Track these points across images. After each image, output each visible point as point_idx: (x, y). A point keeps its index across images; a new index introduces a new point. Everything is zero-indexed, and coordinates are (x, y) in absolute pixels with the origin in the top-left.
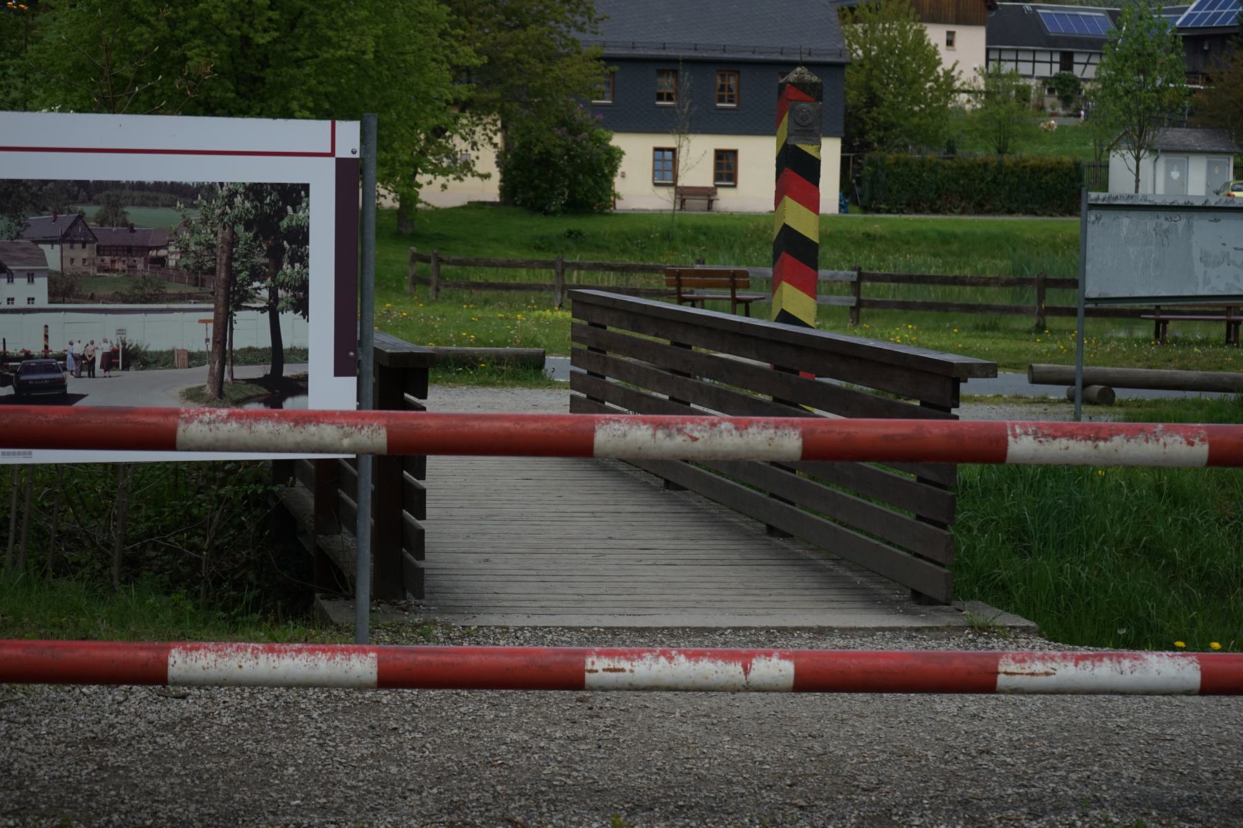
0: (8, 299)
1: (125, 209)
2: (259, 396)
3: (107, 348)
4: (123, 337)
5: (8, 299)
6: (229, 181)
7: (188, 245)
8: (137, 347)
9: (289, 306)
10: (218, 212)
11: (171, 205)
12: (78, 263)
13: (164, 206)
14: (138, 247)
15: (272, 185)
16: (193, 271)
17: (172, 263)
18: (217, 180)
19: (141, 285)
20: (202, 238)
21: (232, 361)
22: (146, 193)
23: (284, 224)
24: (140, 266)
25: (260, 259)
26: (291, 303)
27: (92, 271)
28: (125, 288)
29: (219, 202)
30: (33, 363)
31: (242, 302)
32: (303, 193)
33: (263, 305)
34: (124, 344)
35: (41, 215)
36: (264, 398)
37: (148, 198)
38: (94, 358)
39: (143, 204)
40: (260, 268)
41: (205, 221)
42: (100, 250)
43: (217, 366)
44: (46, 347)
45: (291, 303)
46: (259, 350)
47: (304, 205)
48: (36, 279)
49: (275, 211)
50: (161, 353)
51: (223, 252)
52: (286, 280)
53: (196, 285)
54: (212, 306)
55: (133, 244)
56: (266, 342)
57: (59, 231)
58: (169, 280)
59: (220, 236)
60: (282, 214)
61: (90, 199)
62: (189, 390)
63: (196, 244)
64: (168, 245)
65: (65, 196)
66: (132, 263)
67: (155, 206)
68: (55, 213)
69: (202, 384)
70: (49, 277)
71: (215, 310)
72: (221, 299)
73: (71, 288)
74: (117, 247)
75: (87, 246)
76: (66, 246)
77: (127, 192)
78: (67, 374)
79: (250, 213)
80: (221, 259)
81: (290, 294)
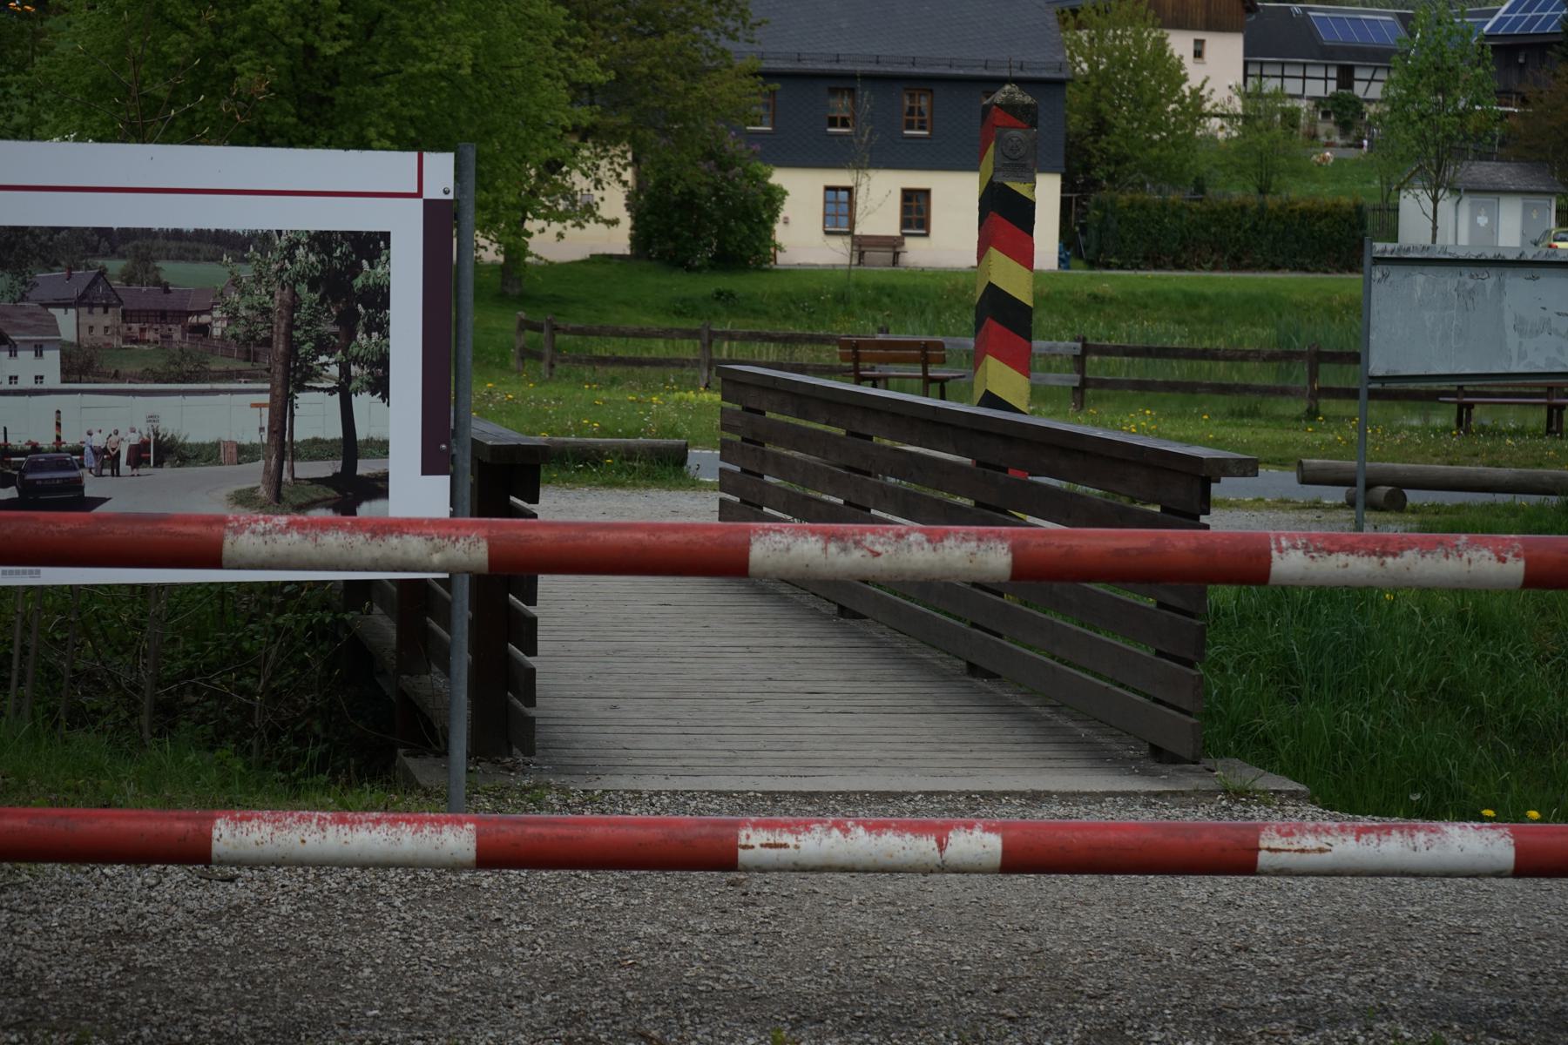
0: (11, 378)
1: (158, 264)
2: (326, 499)
3: (135, 439)
4: (155, 425)
5: (11, 378)
6: (289, 228)
7: (237, 309)
8: (173, 438)
9: (364, 386)
10: (275, 267)
11: (216, 258)
12: (98, 332)
13: (207, 260)
14: (174, 311)
15: (343, 233)
16: (244, 342)
17: (217, 332)
18: (274, 228)
19: (178, 360)
20: (255, 301)
21: (293, 456)
22: (185, 244)
23: (359, 282)
24: (177, 336)
25: (328, 327)
26: (368, 383)
27: (117, 342)
28: (158, 364)
29: (276, 255)
30: (41, 458)
31: (305, 381)
32: (382, 243)
33: (332, 384)
34: (157, 434)
35: (52, 271)
36: (333, 502)
37: (186, 250)
38: (119, 452)
39: (180, 258)
40: (328, 338)
41: (258, 280)
42: (127, 316)
43: (273, 462)
44: (58, 438)
45: (368, 383)
46: (327, 442)
47: (383, 258)
48: (45, 353)
49: (346, 266)
50: (203, 446)
51: (282, 318)
52: (361, 354)
53: (247, 360)
54: (268, 386)
55: (168, 308)
56: (336, 432)
57: (75, 291)
58: (213, 353)
59: (277, 297)
60: (355, 270)
61: (113, 252)
62: (239, 492)
63: (247, 307)
64: (212, 309)
65: (82, 247)
66: (167, 332)
67: (196, 260)
68: (70, 269)
69: (255, 485)
70: (61, 350)
71: (271, 391)
72: (279, 378)
73: (90, 363)
74: (147, 311)
75: (110, 310)
76: (83, 310)
77: (161, 242)
78: (84, 473)
79: (316, 268)
80: (279, 327)
81: (366, 371)
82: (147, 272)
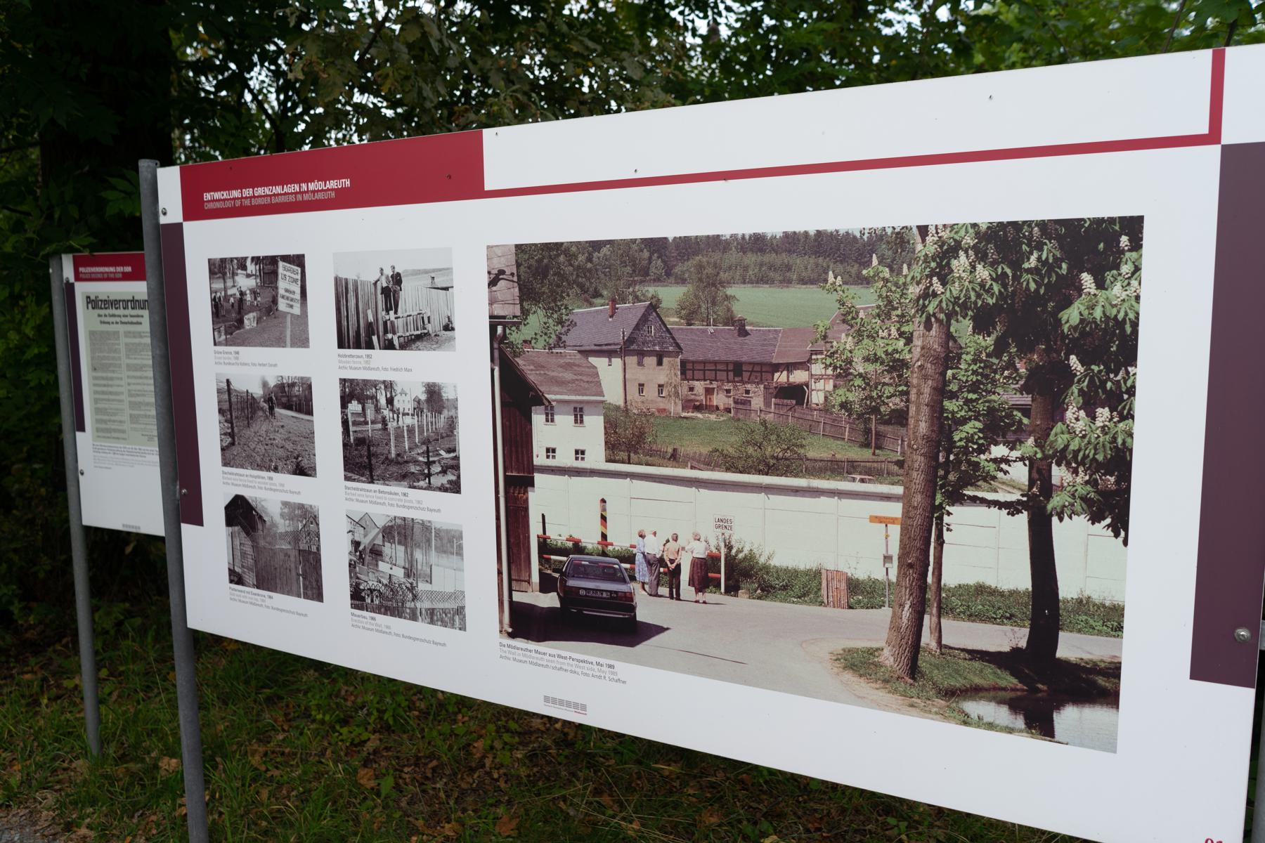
0: (548, 450)
1: (730, 291)
2: (996, 688)
3: (700, 551)
4: (727, 533)
5: (548, 450)
6: (940, 223)
7: (849, 362)
8: (751, 557)
9: (1078, 507)
10: (914, 290)
11: (817, 279)
12: (651, 392)
13: (803, 281)
14: (754, 364)
15: (1043, 225)
16: (860, 416)
17: (817, 398)
18: (914, 222)
19: (758, 438)
20: (880, 348)
21: (940, 608)
22: (769, 258)
23: (1072, 316)
24: (757, 402)
25: (1009, 396)
26: (1084, 499)
27: (675, 407)
28: (730, 443)
29: (917, 270)
30: (585, 560)
31: (965, 486)
32: (1124, 240)
33: (1015, 496)
35: (591, 305)
36: (1012, 695)
37: (771, 267)
38: (679, 566)
39: (761, 280)
40: (1010, 416)
41: (884, 314)
42: (687, 370)
43: (906, 612)
44: (604, 536)
45: (1084, 499)
46: (1002, 594)
47: (1126, 269)
49: (1048, 286)
50: (794, 574)
51: (925, 377)
52: (1074, 446)
55: (745, 359)
56: (1019, 578)
57: (617, 333)
58: (811, 431)
59: (918, 342)
60: (1067, 291)
61: (668, 274)
62: (850, 651)
63: (867, 359)
64: (810, 360)
65: (629, 269)
67: (787, 282)
68: (614, 301)
69: (875, 645)
70: (606, 416)
71: (905, 499)
72: (918, 478)
73: (641, 436)
74: (715, 363)
75: (665, 360)
77: (733, 256)
78: (635, 587)
79: (989, 291)
80: (919, 393)
81: (1082, 477)
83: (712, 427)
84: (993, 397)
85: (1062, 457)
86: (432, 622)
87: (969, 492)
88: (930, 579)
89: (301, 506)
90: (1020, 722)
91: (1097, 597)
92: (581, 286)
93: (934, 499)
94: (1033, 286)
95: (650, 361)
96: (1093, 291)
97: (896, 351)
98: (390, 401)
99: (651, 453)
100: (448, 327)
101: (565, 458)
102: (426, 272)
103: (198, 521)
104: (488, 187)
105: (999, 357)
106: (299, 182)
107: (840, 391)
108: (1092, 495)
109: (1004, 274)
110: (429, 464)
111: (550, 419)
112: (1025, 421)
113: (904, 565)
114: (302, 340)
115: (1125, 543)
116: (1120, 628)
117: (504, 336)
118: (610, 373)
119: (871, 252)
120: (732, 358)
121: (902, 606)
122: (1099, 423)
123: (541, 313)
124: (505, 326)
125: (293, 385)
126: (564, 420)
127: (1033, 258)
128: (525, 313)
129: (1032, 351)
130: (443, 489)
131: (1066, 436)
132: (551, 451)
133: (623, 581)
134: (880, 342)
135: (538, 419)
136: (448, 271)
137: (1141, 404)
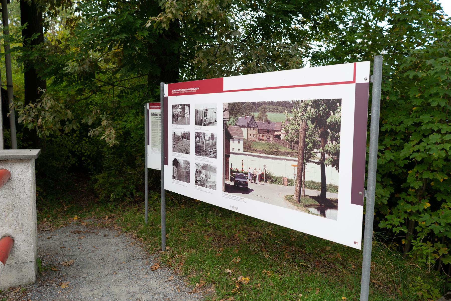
1: (267, 114)
7: (288, 130)
8: (269, 174)
9: (330, 164)
10: (300, 114)
11: (282, 112)
12: (252, 136)
13: (280, 112)
14: (271, 130)
15: (323, 100)
16: (290, 142)
17: (282, 138)
18: (300, 99)
19: (271, 147)
20: (294, 127)
21: (304, 186)
22: (274, 107)
23: (329, 120)
24: (271, 139)
25: (317, 138)
26: (331, 161)
27: (256, 140)
28: (266, 148)
30: (239, 174)
32: (338, 104)
33: (318, 161)
34: (266, 172)
35: (242, 116)
36: (317, 206)
39: (273, 111)
40: (317, 142)
41: (295, 119)
42: (259, 131)
43: (298, 187)
44: (243, 169)
45: (331, 161)
47: (338, 110)
50: (277, 178)
52: (329, 150)
53: (291, 149)
54: (297, 159)
55: (269, 129)
56: (319, 180)
57: (246, 123)
58: (281, 145)
59: (301, 126)
60: (327, 115)
61: (256, 110)
63: (291, 129)
65: (249, 109)
66: (269, 137)
67: (277, 112)
68: (246, 116)
69: (292, 195)
71: (298, 161)
72: (300, 156)
73: (250, 146)
74: (264, 130)
75: (255, 129)
76: (249, 129)
79: (314, 115)
80: (301, 137)
81: (331, 157)
82: (264, 116)
83: (263, 144)
84: (314, 138)
85: (327, 152)
86: (210, 188)
87: (310, 160)
88: (302, 179)
89: (187, 161)
90: (319, 213)
91: (333, 184)
92: (240, 112)
93: (303, 161)
94: (322, 114)
95: (252, 129)
96: (333, 115)
97: (297, 128)
98: (204, 137)
99: (252, 150)
100: (216, 121)
101: (236, 151)
102: (212, 108)
103: (167, 164)
104: (224, 90)
105: (315, 129)
106: (190, 88)
107: (287, 136)
108: (332, 161)
109: (316, 111)
110: (211, 152)
111: (233, 142)
112: (320, 144)
113: (298, 176)
114: (189, 124)
115: (339, 172)
116: (338, 191)
117: (226, 123)
118: (244, 131)
119: (293, 106)
120: (267, 129)
121: (297, 185)
122: (334, 145)
123: (233, 118)
124: (226, 120)
125: (186, 133)
126: (236, 142)
127: (322, 107)
128: (230, 118)
129: (321, 128)
130: (213, 157)
131: (328, 147)
132: (233, 149)
133: (246, 179)
134: (294, 126)
135: (231, 142)
136: (216, 108)
137: (341, 140)
